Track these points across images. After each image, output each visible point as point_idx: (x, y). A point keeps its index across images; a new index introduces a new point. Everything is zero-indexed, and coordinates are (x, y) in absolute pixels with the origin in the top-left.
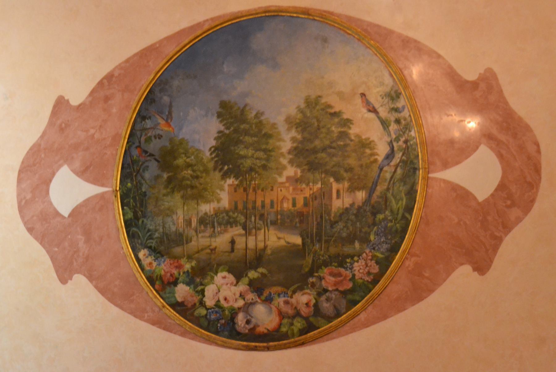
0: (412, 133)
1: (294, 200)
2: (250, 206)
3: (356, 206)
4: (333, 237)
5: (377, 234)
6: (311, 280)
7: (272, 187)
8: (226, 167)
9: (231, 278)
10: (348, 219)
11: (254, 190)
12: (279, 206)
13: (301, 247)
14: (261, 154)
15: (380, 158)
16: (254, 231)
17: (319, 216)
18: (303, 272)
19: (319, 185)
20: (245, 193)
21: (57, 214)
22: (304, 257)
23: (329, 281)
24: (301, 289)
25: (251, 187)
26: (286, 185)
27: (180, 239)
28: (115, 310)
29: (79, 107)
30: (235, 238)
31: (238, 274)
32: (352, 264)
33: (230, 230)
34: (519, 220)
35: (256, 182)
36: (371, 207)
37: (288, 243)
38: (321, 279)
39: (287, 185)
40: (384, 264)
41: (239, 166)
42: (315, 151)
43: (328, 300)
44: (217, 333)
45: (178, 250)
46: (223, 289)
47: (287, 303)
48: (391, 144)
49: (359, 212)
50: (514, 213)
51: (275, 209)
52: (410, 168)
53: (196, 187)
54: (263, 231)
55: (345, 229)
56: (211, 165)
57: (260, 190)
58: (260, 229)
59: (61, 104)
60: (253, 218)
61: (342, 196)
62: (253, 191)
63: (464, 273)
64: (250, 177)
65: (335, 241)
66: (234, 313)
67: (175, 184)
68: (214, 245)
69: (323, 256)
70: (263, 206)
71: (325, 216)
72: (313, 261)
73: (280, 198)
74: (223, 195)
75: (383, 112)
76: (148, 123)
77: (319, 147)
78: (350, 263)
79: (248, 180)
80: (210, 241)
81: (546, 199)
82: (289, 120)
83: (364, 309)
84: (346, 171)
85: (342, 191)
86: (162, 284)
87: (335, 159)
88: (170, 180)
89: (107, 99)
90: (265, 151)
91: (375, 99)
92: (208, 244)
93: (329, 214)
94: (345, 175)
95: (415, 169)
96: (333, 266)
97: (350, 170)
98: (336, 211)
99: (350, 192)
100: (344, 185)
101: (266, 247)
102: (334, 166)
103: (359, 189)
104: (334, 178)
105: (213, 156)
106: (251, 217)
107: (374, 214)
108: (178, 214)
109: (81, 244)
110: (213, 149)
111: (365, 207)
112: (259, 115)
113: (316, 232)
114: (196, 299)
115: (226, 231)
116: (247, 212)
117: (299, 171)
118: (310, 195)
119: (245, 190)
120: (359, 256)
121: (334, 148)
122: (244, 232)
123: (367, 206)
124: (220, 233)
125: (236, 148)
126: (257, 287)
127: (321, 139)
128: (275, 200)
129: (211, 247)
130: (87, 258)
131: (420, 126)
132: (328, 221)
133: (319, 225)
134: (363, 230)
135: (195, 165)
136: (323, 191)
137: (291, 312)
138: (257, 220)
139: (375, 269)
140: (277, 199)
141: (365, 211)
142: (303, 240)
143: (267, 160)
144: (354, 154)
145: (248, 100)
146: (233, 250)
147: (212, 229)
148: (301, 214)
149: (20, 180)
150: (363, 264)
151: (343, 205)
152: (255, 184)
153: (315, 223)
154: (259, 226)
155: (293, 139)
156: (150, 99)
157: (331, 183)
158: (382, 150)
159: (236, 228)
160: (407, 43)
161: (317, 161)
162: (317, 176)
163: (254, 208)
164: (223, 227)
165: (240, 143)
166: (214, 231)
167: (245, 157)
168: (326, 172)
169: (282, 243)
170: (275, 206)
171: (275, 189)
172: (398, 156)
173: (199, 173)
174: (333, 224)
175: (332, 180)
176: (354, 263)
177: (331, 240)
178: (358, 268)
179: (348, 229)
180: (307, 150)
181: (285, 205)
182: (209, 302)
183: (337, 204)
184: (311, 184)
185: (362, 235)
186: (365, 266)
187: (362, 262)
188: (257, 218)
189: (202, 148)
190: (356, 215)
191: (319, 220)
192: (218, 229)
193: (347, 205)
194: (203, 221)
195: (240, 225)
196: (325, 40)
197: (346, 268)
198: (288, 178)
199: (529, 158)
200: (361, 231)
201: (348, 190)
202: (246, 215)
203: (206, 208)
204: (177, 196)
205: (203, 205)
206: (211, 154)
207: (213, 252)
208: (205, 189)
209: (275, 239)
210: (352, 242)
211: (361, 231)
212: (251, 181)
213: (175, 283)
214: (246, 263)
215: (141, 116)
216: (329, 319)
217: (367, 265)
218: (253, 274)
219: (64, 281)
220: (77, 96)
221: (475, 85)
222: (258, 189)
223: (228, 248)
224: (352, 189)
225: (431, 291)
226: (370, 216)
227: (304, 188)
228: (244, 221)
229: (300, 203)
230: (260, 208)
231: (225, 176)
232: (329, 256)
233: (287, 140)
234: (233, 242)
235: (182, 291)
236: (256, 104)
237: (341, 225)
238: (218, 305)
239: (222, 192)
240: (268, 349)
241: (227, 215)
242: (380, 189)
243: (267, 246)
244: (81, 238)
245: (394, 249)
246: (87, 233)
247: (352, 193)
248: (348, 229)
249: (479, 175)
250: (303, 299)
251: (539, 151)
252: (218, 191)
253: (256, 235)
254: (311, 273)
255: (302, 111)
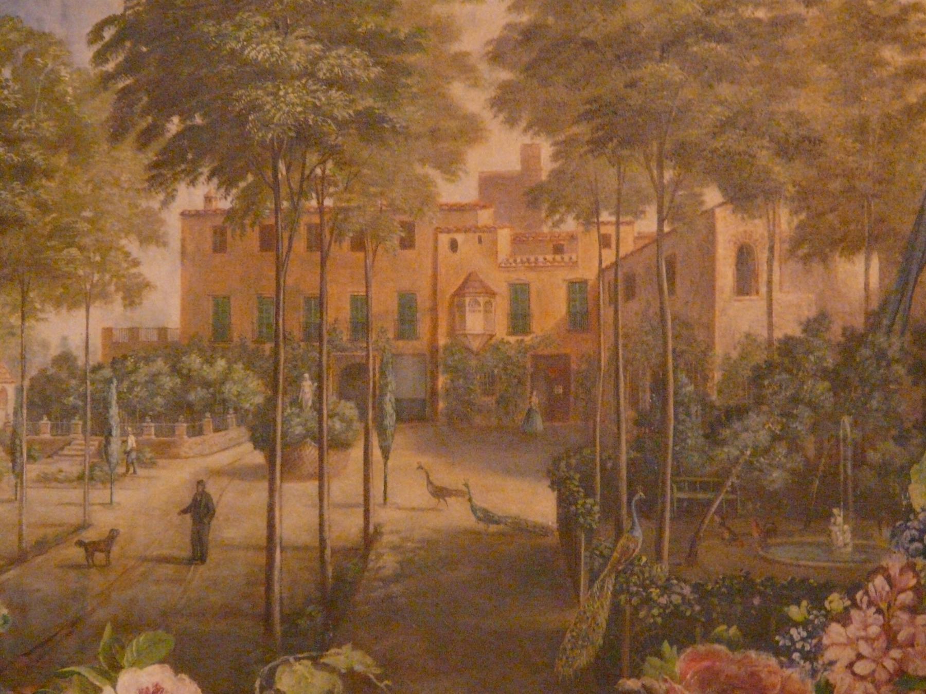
1: (520, 293)
2: (294, 322)
3: (836, 333)
4: (717, 487)
7: (409, 228)
8: (174, 125)
10: (795, 400)
11: (317, 243)
12: (443, 329)
13: (553, 540)
16: (310, 452)
17: (647, 382)
18: (564, 670)
19: (648, 224)
20: (270, 256)
22: (565, 590)
25: (303, 229)
30: (212, 489)
32: (814, 631)
33: (188, 444)
35: (328, 202)
36: (908, 337)
37: (487, 517)
39: (485, 217)
41: (241, 119)
42: (626, 49)
51: (421, 344)
53: (19, 222)
54: (356, 453)
55: (781, 449)
56: (98, 112)
57: (346, 244)
58: (342, 445)
60: (308, 387)
61: (763, 278)
62: (310, 248)
64: (297, 177)
65: (729, 511)
68: (104, 520)
69: (666, 589)
70: (361, 326)
71: (681, 384)
72: (616, 610)
73: (449, 287)
74: (160, 267)
77: (646, 29)
78: (805, 624)
79: (284, 191)
80: (85, 504)
84: (785, 150)
85: (762, 256)
87: (725, 90)
92: (72, 515)
94: (781, 172)
96: (719, 640)
97: (801, 145)
98: (735, 355)
99: (806, 259)
100: (773, 224)
101: (369, 538)
102: (723, 126)
103: (852, 245)
104: (724, 190)
105: (110, 67)
106: (295, 382)
110: (109, 34)
111: (881, 339)
113: (631, 463)
115: (165, 450)
116: (275, 352)
117: (546, 149)
118: (602, 271)
119: (269, 239)
120: (850, 591)
121: (723, 37)
122: (259, 458)
123: (889, 332)
124: (133, 461)
125: (227, 26)
128: (423, 300)
129: (89, 536)
132: (694, 409)
133: (649, 425)
134: (873, 456)
135: (17, 112)
136: (666, 251)
138: (330, 397)
140: (435, 292)
141: (881, 355)
142: (564, 502)
144: (822, 69)
146: (199, 554)
147: (95, 443)
148: (553, 370)
150: (874, 630)
151: (771, 326)
152: (321, 210)
153: (627, 413)
154: (338, 425)
157: (710, 214)
159: (219, 438)
161: (635, 99)
162: (640, 175)
163: (315, 333)
164: (151, 431)
166: (104, 452)
168: (683, 154)
169: (457, 515)
170: (423, 327)
171: (423, 235)
173: (37, 155)
174: (718, 423)
175: (712, 196)
176: (824, 627)
177: (709, 503)
178: (848, 654)
179: (795, 446)
180: (588, 44)
181: (474, 323)
183: (740, 321)
184: (605, 216)
185: (869, 479)
186: (881, 643)
188: (331, 386)
189: (52, 25)
190: (838, 380)
191: (646, 398)
192: (124, 440)
193: (789, 327)
195: (241, 422)
197: (784, 653)
200: (860, 461)
201: (792, 252)
203: (67, 331)
205: (50, 313)
206: (100, 57)
207: (99, 557)
208: (65, 235)
209: (416, 496)
210: (815, 516)
211: (860, 461)
212: (302, 193)
214: (267, 618)
217: (890, 635)
222: (338, 234)
223: (175, 537)
224: (817, 245)
226: (908, 381)
227: (572, 237)
228: (259, 400)
229: (552, 310)
230: (345, 337)
231: (167, 169)
232: (696, 588)
234: (200, 509)
237: (756, 429)
239: (153, 249)
241: (175, 370)
243: (378, 533)
247: (817, 267)
248: (795, 446)
252: (131, 245)
253: (321, 477)
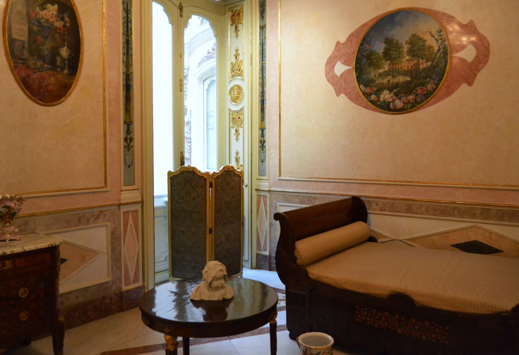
0: (446, 43)
5: (435, 75)
6: (414, 91)
9: (388, 92)
14: (398, 53)
15: (436, 51)
21: (336, 76)
22: (411, 84)
23: (419, 91)
24: (410, 94)
26: (406, 62)
27: (373, 81)
28: (353, 104)
29: (344, 44)
31: (391, 91)
34: (483, 68)
38: (417, 91)
40: (437, 85)
43: (419, 97)
44: (384, 109)
45: (372, 84)
46: (386, 96)
47: (406, 99)
48: (439, 47)
49: (428, 69)
50: (481, 65)
52: (445, 53)
56: (382, 57)
59: (338, 43)
63: (464, 87)
66: (389, 103)
67: (371, 64)
74: (386, 66)
75: (436, 37)
76: (363, 47)
81: (493, 60)
82: (406, 42)
83: (431, 99)
86: (367, 95)
88: (370, 63)
89: (351, 40)
90: (399, 52)
91: (434, 32)
93: (419, 70)
95: (447, 54)
97: (426, 55)
103: (429, 61)
107: (434, 69)
108: (373, 73)
109: (343, 84)
112: (397, 41)
114: (377, 99)
126: (396, 94)
127: (417, 47)
130: (345, 88)
131: (448, 40)
137: (407, 102)
139: (434, 86)
143: (400, 54)
145: (394, 37)
146: (389, 83)
149: (326, 67)
155: (408, 48)
156: (364, 39)
158: (436, 48)
160: (444, 14)
165: (392, 49)
167: (393, 54)
168: (419, 57)
169: (404, 80)
172: (442, 50)
182: (381, 100)
183: (422, 67)
187: (430, 85)
192: (384, 77)
194: (380, 75)
196: (417, 16)
198: (406, 60)
199: (486, 47)
202: (393, 72)
203: (381, 71)
204: (372, 68)
209: (402, 79)
213: (371, 95)
215: (362, 45)
216: (419, 103)
218: (395, 91)
219: (338, 96)
220: (343, 40)
221: (466, 26)
223: (387, 82)
224: (427, 62)
225: (453, 92)
229: (410, 67)
231: (387, 60)
233: (406, 48)
234: (389, 81)
235: (373, 97)
236: (396, 38)
237: (423, 73)
238: (384, 101)
240: (400, 114)
242: (436, 61)
244: (343, 82)
245: (441, 80)
246: (345, 81)
249: (469, 54)
250: (411, 97)
251: (489, 45)
254: (413, 89)
255: (410, 38)
